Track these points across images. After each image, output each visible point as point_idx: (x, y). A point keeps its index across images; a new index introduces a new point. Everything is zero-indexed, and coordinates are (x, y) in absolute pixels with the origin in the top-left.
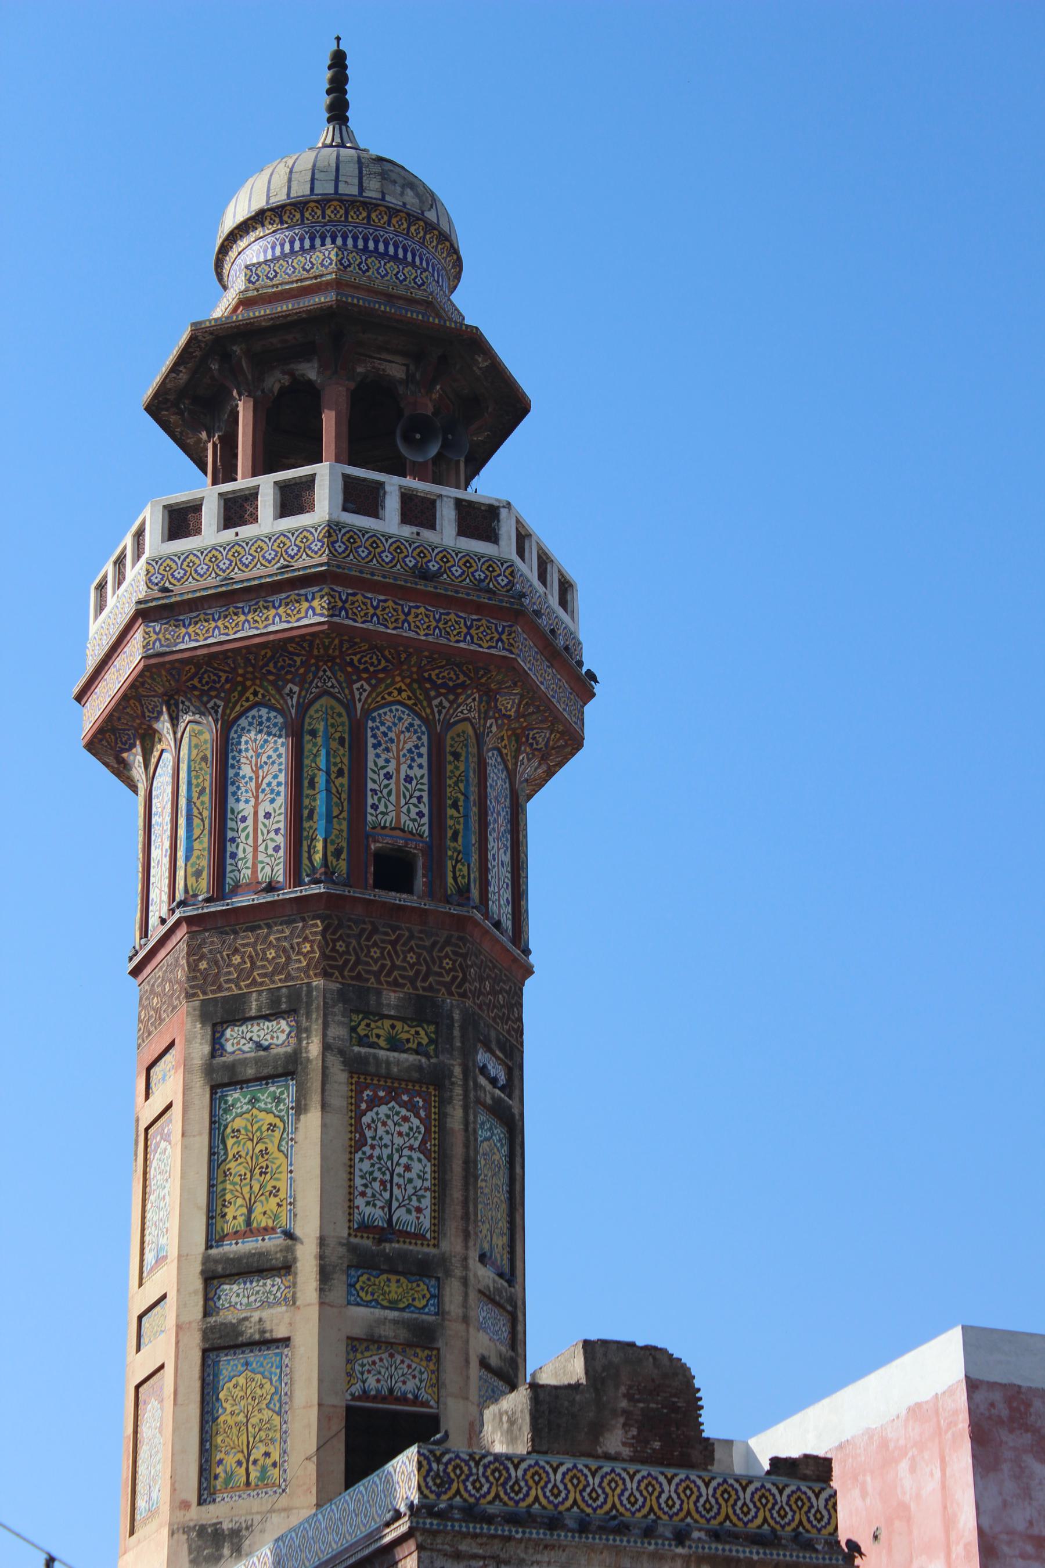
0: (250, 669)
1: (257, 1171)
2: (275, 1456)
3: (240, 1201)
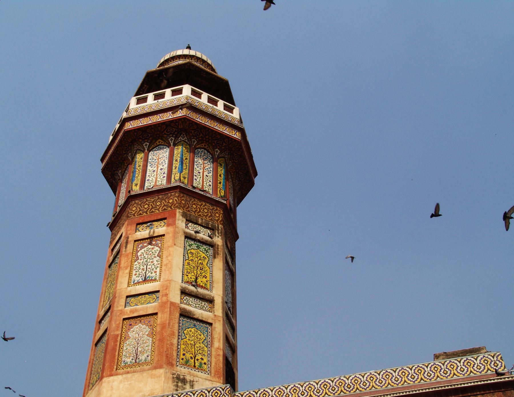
0: (210, 138)
2: (205, 360)
3: (193, 274)
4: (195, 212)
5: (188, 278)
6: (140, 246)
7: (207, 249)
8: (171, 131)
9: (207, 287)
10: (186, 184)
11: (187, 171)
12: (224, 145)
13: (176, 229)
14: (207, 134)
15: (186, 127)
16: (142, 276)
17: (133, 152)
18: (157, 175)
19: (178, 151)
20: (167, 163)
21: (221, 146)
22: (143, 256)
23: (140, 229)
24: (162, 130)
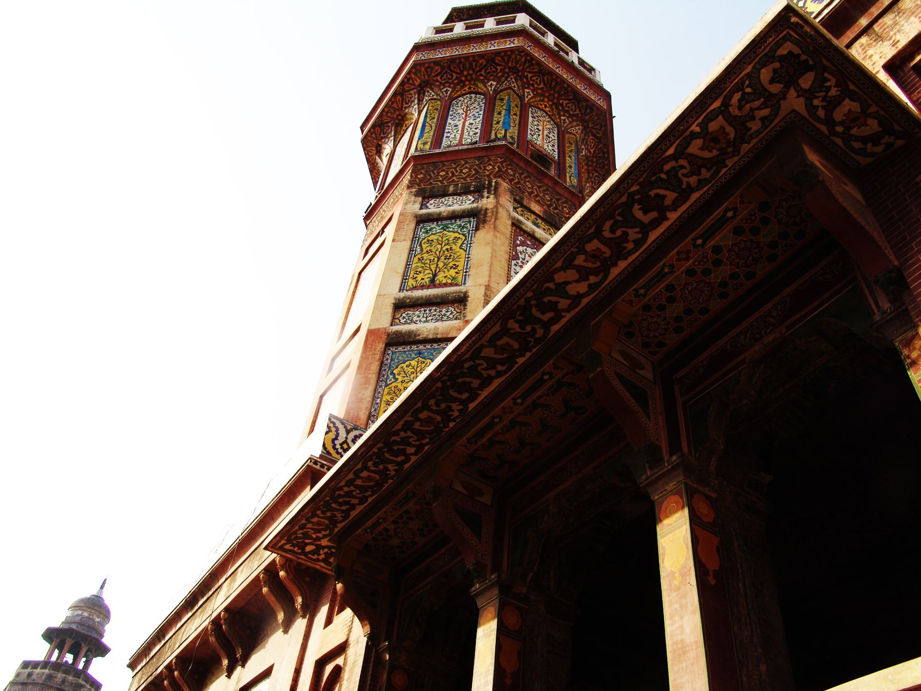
0: (471, 72)
1: (443, 258)
9: (455, 283)
12: (499, 71)
21: (495, 74)
24: (400, 105)
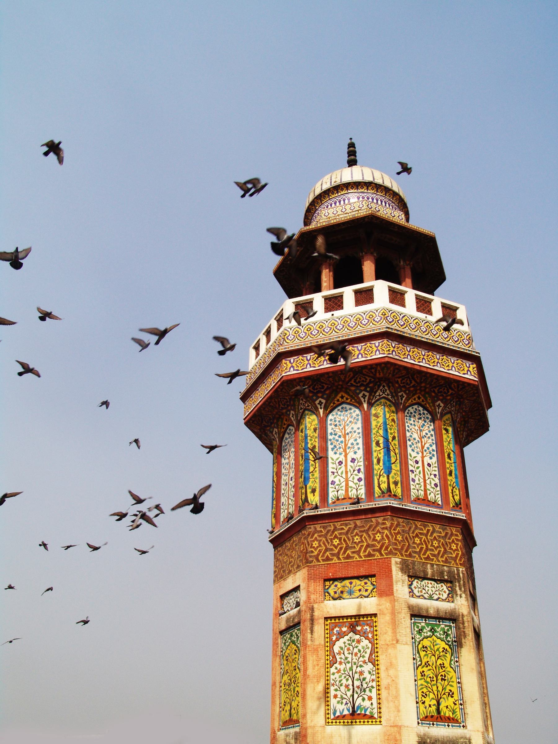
0: (428, 386)
4: (419, 553)
5: (426, 708)
6: (335, 631)
7: (446, 628)
8: (363, 381)
10: (400, 497)
11: (398, 465)
12: (449, 394)
13: (395, 605)
14: (422, 380)
15: (389, 375)
16: (346, 704)
17: (298, 411)
18: (347, 472)
19: (378, 422)
20: (361, 445)
21: (445, 395)
22: (342, 656)
23: (331, 591)
24: (347, 379)
